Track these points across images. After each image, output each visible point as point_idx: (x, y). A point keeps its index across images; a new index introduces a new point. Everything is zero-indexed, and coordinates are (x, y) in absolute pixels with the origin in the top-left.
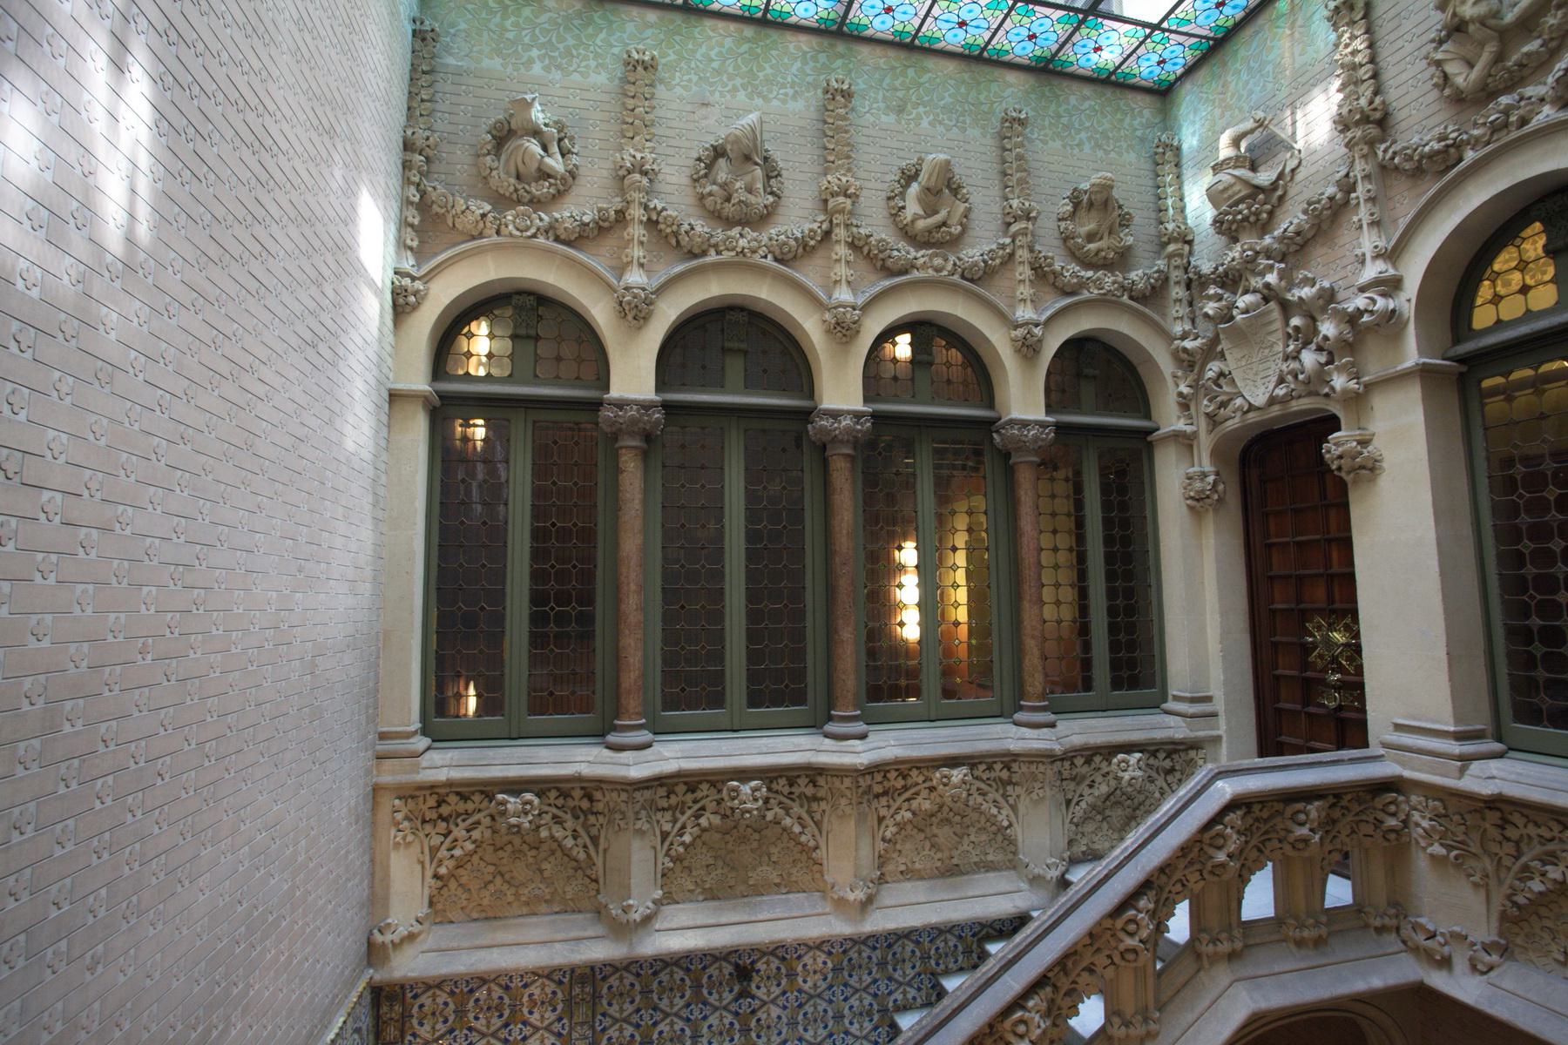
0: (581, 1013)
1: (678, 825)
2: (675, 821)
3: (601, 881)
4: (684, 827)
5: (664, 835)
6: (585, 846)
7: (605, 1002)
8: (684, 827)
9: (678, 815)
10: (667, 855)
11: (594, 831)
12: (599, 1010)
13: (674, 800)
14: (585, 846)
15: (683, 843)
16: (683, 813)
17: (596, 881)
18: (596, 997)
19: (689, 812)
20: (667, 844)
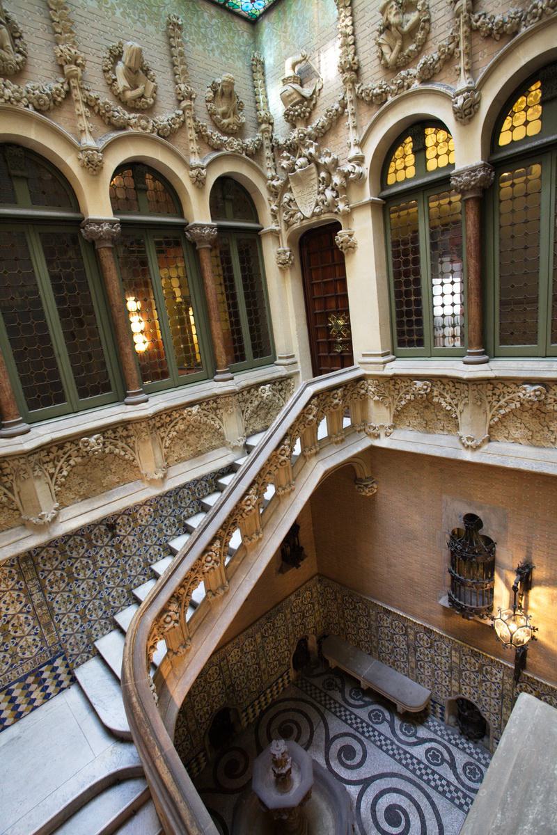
0: (29, 575)
1: (58, 468)
2: (55, 467)
3: (21, 509)
4: (61, 468)
5: (52, 475)
6: (5, 494)
7: (41, 565)
8: (61, 468)
9: (56, 463)
10: (56, 484)
11: (8, 485)
12: (39, 569)
13: (52, 456)
14: (5, 494)
15: (64, 476)
16: (59, 461)
17: (17, 510)
18: (36, 565)
19: (62, 460)
20: (54, 479)
